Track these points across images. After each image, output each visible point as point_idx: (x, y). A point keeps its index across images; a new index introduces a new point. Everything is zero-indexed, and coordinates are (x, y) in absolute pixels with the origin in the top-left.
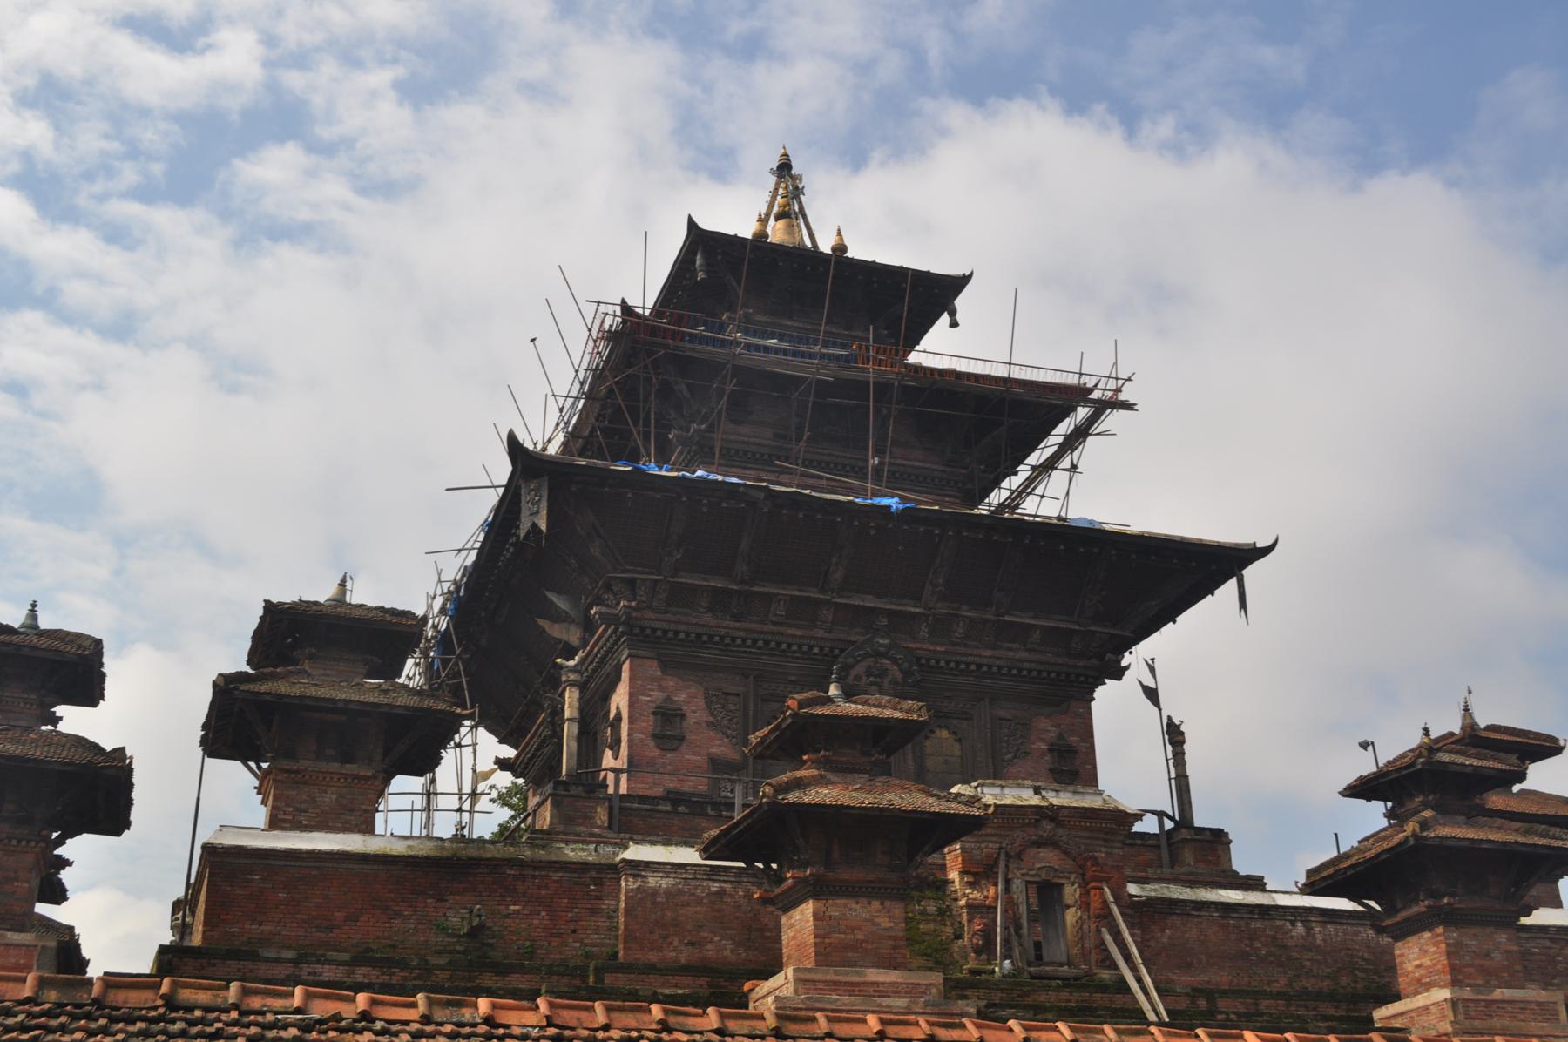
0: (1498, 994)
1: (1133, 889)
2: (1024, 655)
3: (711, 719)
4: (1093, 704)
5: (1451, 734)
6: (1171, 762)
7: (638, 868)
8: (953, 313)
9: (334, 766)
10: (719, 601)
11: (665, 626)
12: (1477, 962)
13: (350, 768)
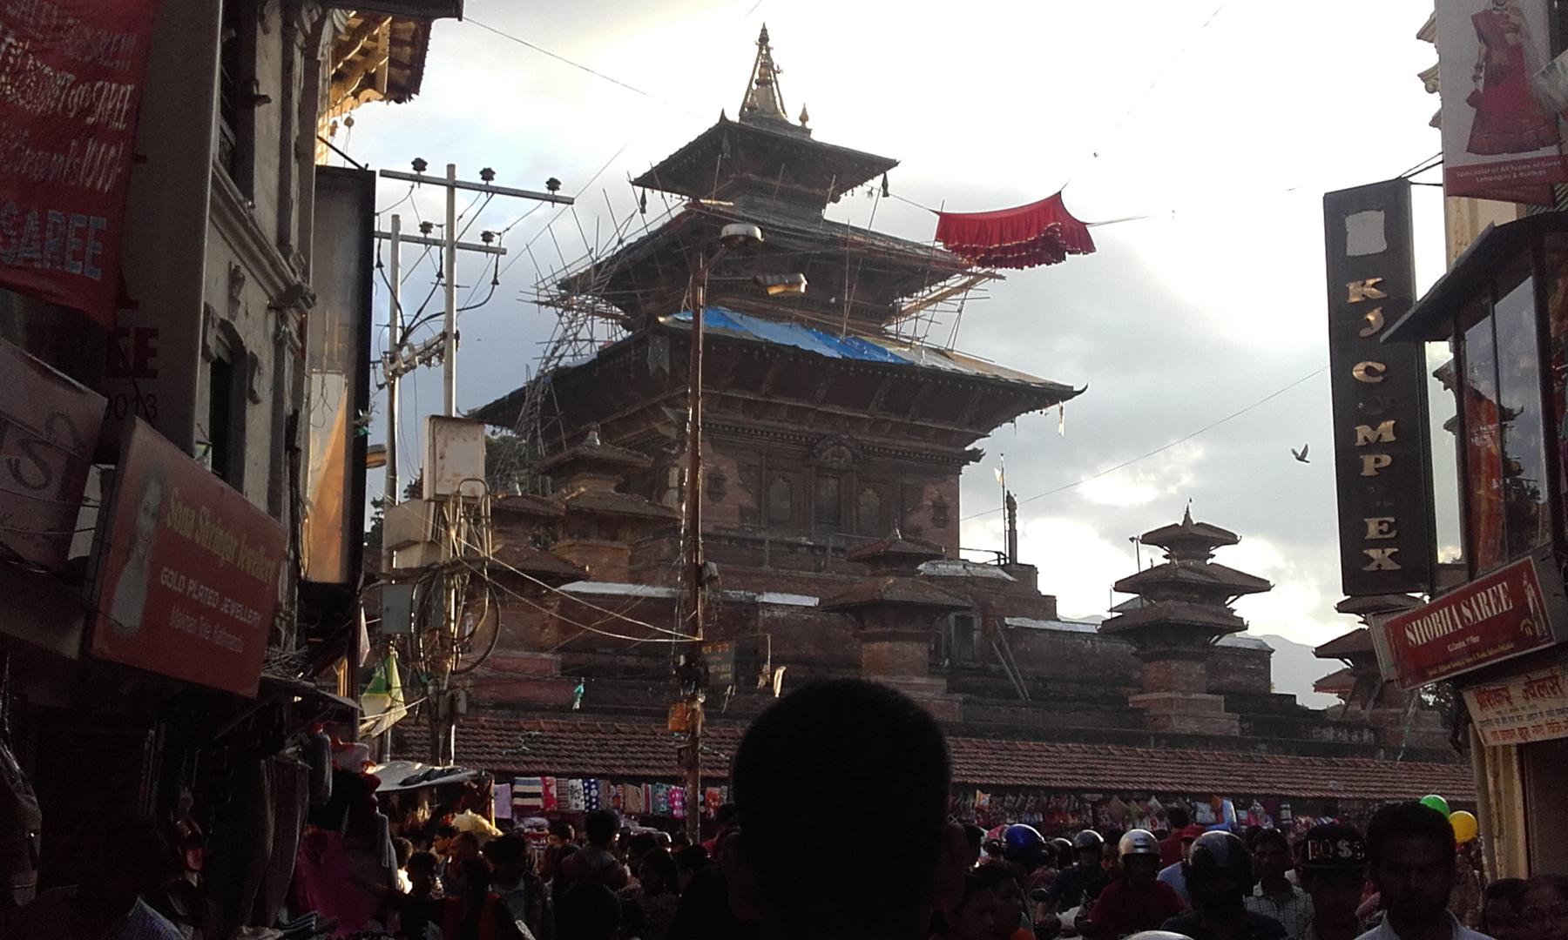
0: (1193, 696)
1: (1007, 621)
2: (923, 445)
3: (741, 482)
4: (961, 476)
5: (1177, 525)
6: (1007, 520)
7: (769, 606)
8: (885, 185)
9: (608, 543)
10: (748, 406)
11: (717, 422)
12: (1185, 678)
13: (616, 544)
